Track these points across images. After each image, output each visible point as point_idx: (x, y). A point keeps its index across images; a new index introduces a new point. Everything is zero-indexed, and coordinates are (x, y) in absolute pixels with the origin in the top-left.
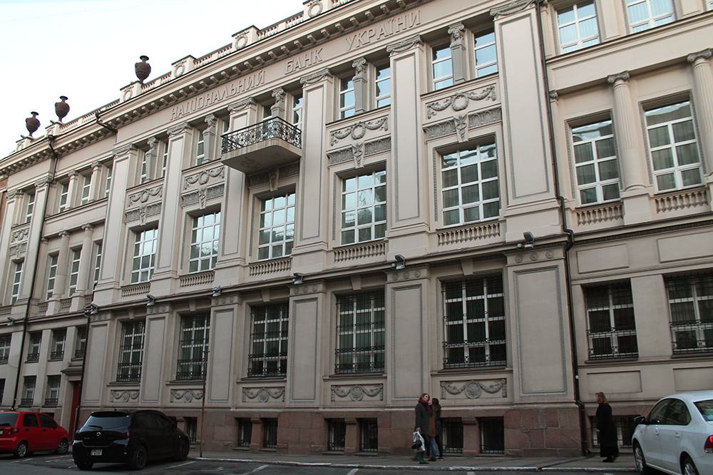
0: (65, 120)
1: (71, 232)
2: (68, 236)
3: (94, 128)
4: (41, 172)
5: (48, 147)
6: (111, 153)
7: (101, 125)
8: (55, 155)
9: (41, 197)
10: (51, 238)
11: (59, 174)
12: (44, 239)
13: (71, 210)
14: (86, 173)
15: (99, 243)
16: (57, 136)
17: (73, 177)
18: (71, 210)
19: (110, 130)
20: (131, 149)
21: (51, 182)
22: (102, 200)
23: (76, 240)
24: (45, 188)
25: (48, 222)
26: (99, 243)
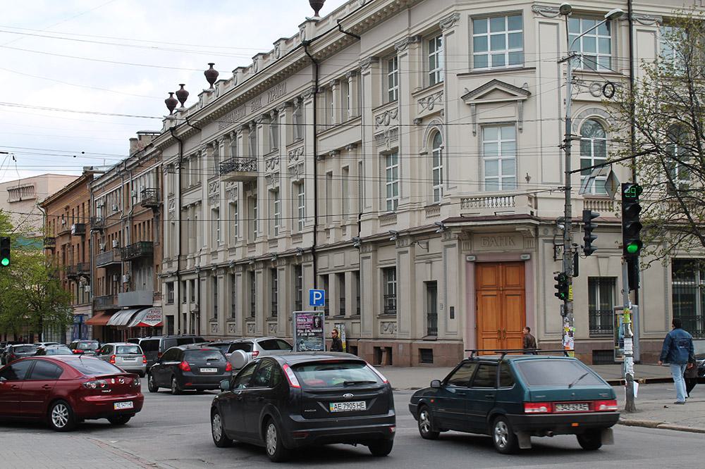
0: (323, 12)
1: (339, 152)
2: (338, 156)
3: (337, 35)
4: (303, 82)
5: (304, 54)
6: (357, 63)
7: (343, 31)
8: (316, 63)
9: (308, 110)
10: (324, 157)
11: (322, 83)
12: (319, 159)
13: (339, 126)
14: (342, 81)
15: (361, 163)
16: (310, 42)
17: (334, 87)
18: (339, 126)
19: (354, 37)
20: (371, 63)
21: (316, 91)
22: (358, 118)
23: (348, 160)
24: (312, 100)
25: (320, 139)
26: (361, 163)
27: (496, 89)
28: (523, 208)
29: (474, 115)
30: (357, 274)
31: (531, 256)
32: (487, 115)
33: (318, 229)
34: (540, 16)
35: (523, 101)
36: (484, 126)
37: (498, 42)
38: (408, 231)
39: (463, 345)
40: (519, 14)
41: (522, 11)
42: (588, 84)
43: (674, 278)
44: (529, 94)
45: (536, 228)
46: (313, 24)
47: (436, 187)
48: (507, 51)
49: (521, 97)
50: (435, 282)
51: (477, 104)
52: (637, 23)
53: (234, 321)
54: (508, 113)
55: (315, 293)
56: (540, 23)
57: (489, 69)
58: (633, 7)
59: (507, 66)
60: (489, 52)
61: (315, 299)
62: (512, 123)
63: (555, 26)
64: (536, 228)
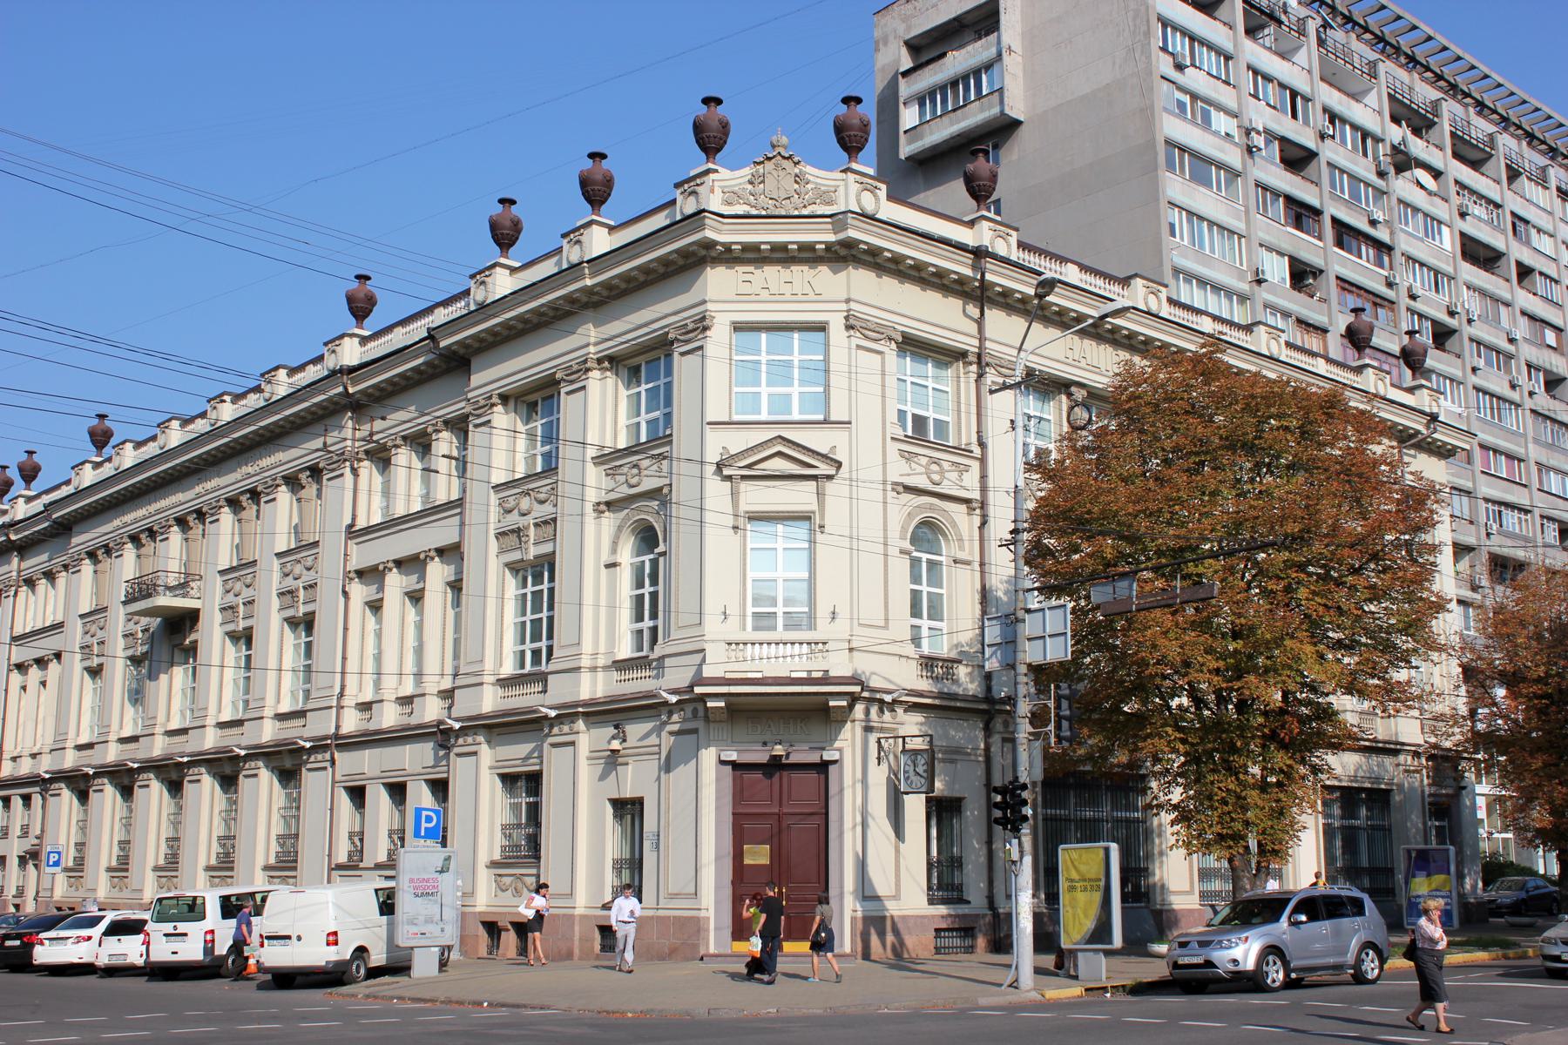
27: (779, 454)
28: (840, 666)
29: (734, 494)
30: (440, 788)
31: (841, 755)
32: (758, 496)
33: (347, 701)
34: (858, 334)
35: (830, 477)
36: (755, 517)
37: (781, 372)
38: (585, 704)
39: (708, 918)
40: (821, 328)
41: (827, 323)
42: (924, 461)
43: (1045, 806)
44: (839, 465)
45: (854, 699)
46: (356, 340)
47: (640, 625)
48: (795, 390)
49: (824, 469)
50: (639, 802)
51: (744, 477)
52: (993, 371)
53: (127, 870)
54: (799, 496)
55: (424, 813)
56: (859, 347)
57: (764, 417)
58: (988, 344)
59: (796, 416)
60: (764, 390)
61: (424, 825)
62: (806, 517)
63: (878, 357)
64: (854, 699)
